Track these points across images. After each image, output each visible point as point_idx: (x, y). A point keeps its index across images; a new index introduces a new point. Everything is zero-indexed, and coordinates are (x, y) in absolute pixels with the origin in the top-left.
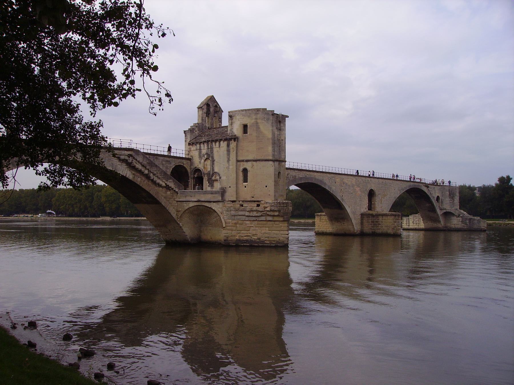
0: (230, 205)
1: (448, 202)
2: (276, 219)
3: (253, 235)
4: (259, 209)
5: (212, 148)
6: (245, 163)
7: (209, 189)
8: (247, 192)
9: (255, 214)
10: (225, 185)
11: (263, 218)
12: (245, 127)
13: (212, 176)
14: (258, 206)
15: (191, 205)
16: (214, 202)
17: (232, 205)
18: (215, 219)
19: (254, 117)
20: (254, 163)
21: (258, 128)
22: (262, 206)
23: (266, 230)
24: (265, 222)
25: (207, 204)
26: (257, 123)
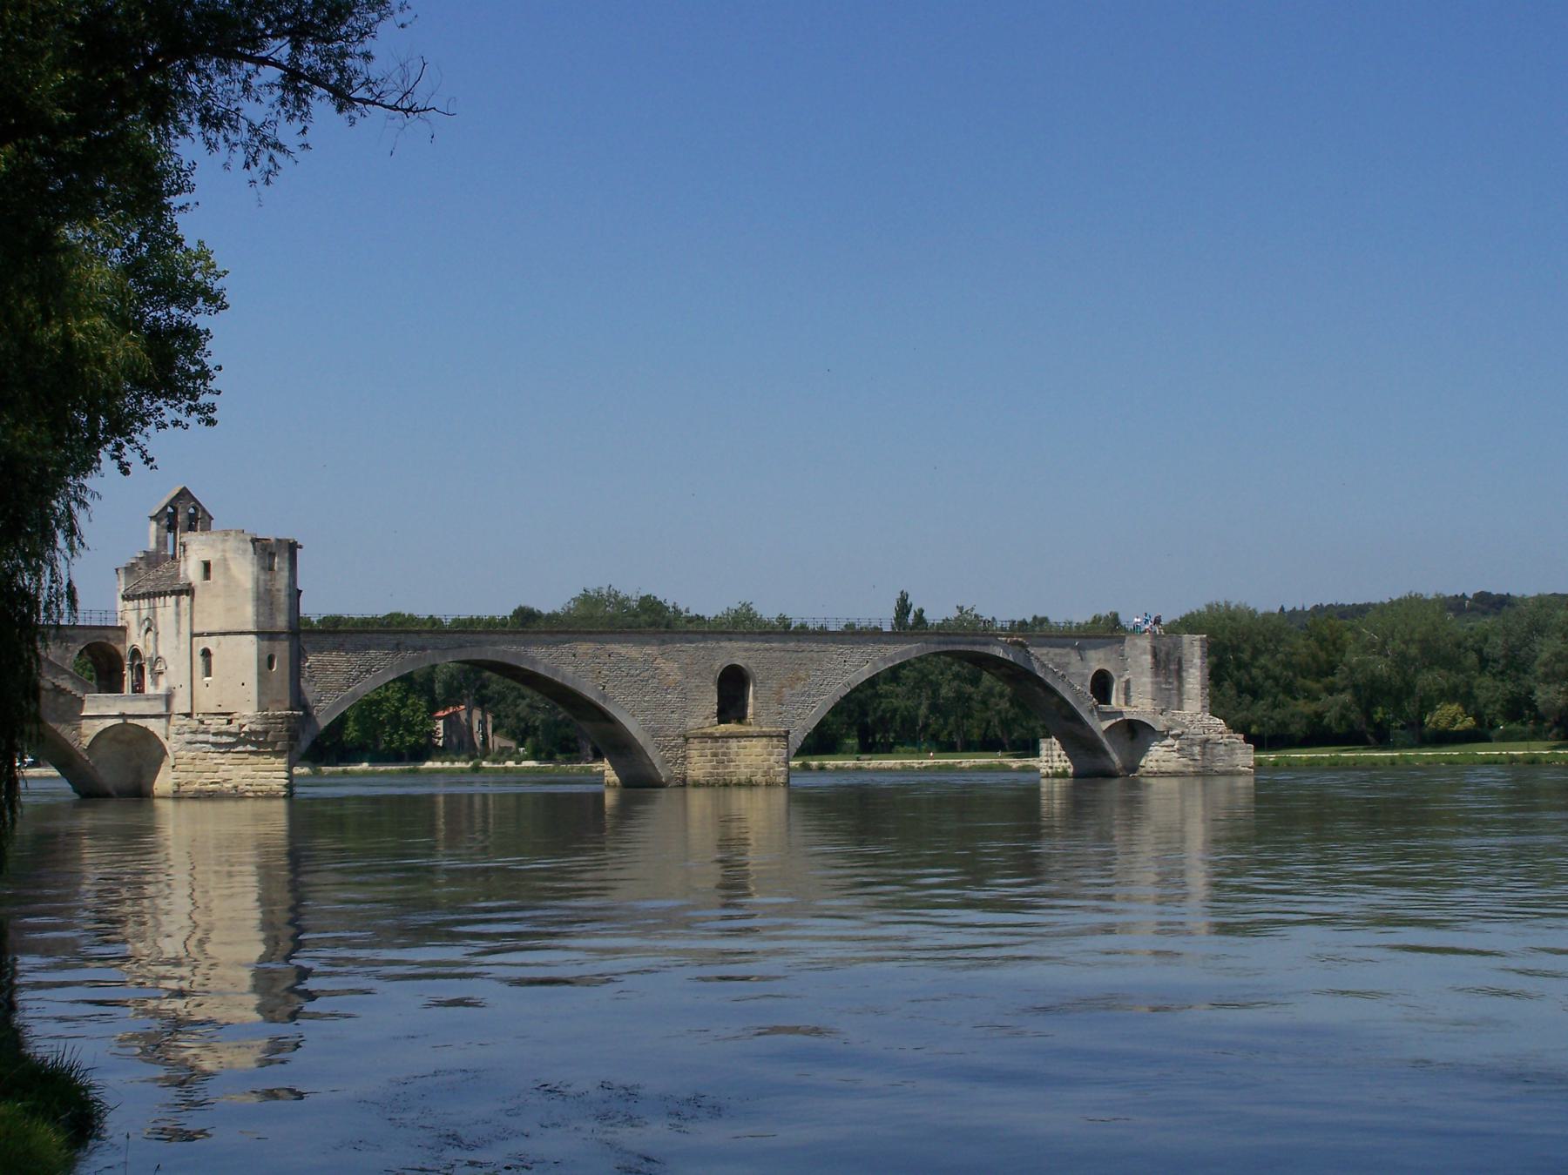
1: (1149, 688)
3: (225, 780)
4: (233, 728)
9: (225, 739)
11: (240, 748)
12: (207, 566)
14: (230, 722)
15: (110, 723)
19: (220, 547)
21: (227, 569)
22: (236, 723)
23: (247, 770)
25: (136, 721)
26: (225, 560)
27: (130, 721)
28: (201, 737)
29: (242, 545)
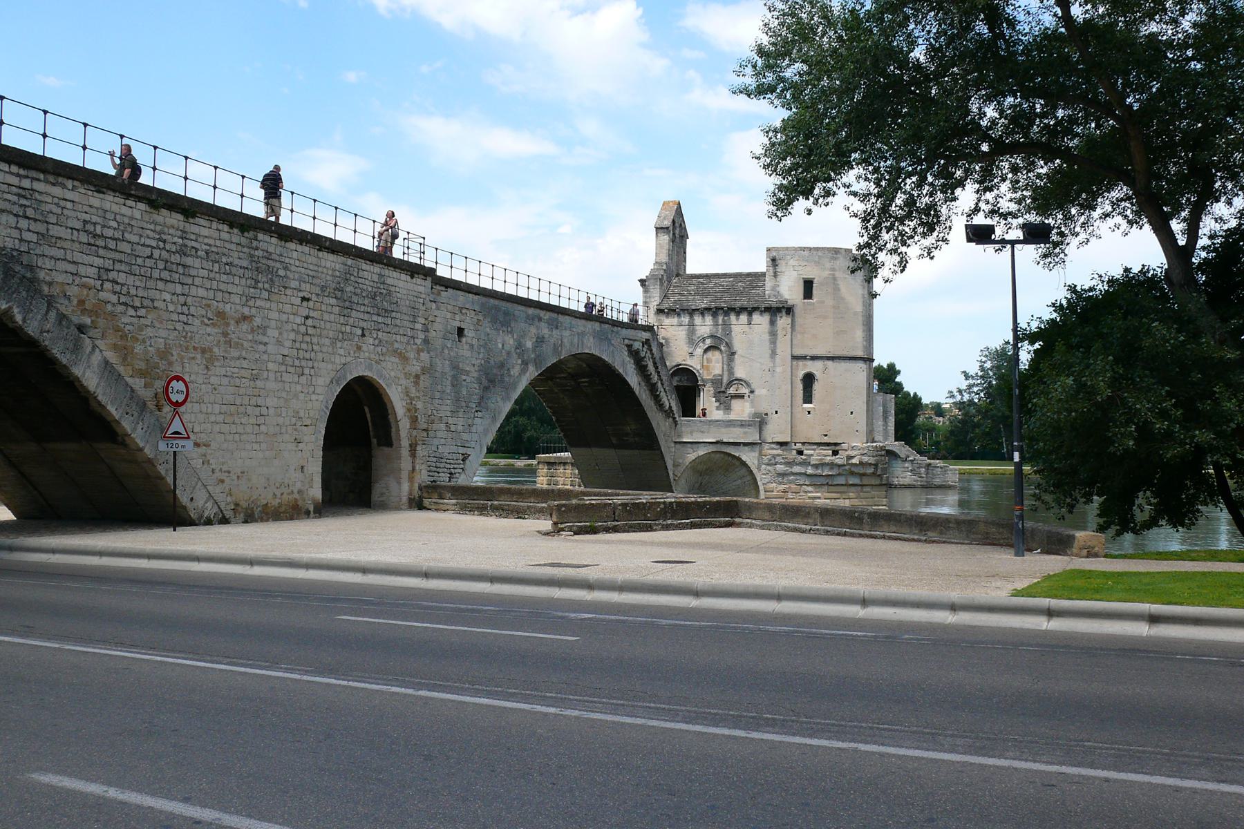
0: (775, 452)
2: (866, 481)
4: (839, 459)
5: (727, 325)
6: (810, 363)
7: (716, 414)
8: (812, 424)
10: (764, 407)
11: (841, 480)
12: (808, 286)
13: (730, 384)
14: (835, 453)
15: (702, 452)
16: (745, 444)
17: (779, 452)
18: (739, 482)
19: (828, 265)
20: (830, 363)
21: (836, 289)
22: (843, 455)
24: (844, 489)
26: (835, 279)
28: (797, 469)
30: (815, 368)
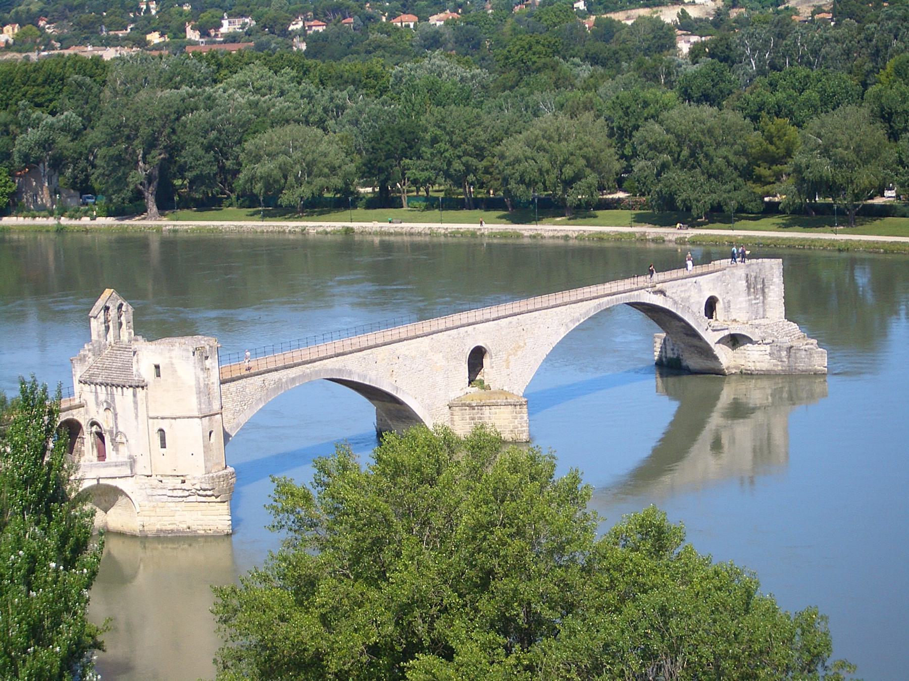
1: (745, 305)
4: (184, 486)
5: (112, 394)
9: (180, 493)
21: (175, 371)
27: (102, 481)
29: (185, 353)
30: (164, 424)
